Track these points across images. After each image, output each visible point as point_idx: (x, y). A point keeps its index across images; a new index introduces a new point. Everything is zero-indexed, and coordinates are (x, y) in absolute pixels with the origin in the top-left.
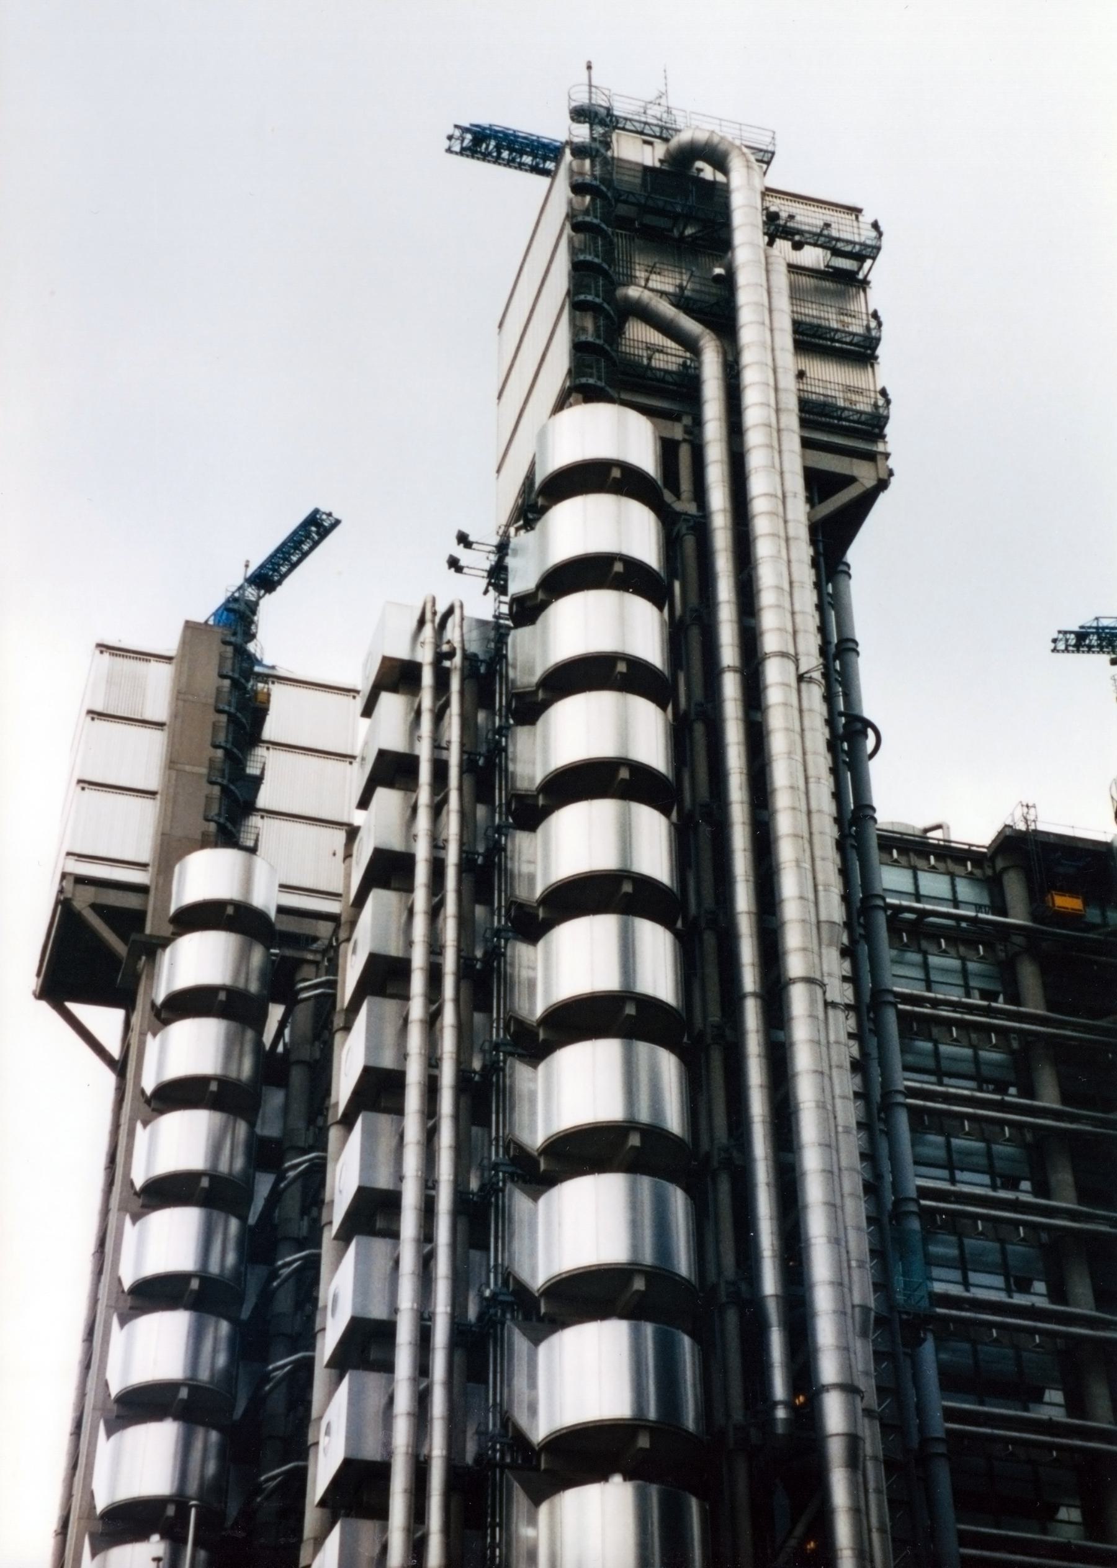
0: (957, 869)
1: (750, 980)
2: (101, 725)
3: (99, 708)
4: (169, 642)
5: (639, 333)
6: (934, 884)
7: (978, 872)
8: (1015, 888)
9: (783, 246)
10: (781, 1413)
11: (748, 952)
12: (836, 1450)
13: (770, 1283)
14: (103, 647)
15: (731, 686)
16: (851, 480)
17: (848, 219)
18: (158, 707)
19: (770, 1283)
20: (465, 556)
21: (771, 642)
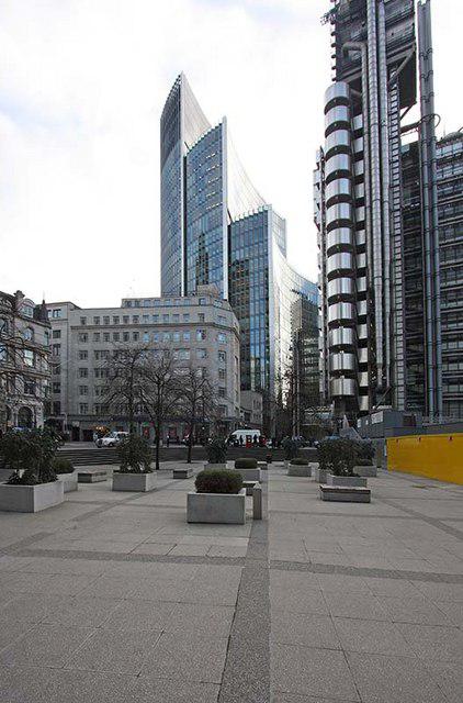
5: (351, 53)
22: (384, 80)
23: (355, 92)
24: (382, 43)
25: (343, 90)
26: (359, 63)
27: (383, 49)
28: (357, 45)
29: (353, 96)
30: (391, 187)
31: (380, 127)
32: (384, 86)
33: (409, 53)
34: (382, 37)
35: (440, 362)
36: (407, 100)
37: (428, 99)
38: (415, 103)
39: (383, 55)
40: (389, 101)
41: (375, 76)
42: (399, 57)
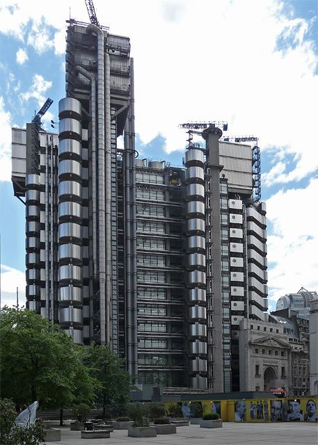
9: (110, 51)
11: (94, 205)
17: (125, 41)
21: (100, 147)
22: (109, 117)
23: (84, 110)
24: (108, 87)
25: (75, 106)
26: (89, 88)
27: (109, 92)
28: (88, 74)
29: (82, 112)
31: (106, 153)
32: (109, 121)
33: (125, 104)
34: (108, 82)
39: (108, 96)
40: (111, 131)
41: (104, 114)
42: (118, 102)
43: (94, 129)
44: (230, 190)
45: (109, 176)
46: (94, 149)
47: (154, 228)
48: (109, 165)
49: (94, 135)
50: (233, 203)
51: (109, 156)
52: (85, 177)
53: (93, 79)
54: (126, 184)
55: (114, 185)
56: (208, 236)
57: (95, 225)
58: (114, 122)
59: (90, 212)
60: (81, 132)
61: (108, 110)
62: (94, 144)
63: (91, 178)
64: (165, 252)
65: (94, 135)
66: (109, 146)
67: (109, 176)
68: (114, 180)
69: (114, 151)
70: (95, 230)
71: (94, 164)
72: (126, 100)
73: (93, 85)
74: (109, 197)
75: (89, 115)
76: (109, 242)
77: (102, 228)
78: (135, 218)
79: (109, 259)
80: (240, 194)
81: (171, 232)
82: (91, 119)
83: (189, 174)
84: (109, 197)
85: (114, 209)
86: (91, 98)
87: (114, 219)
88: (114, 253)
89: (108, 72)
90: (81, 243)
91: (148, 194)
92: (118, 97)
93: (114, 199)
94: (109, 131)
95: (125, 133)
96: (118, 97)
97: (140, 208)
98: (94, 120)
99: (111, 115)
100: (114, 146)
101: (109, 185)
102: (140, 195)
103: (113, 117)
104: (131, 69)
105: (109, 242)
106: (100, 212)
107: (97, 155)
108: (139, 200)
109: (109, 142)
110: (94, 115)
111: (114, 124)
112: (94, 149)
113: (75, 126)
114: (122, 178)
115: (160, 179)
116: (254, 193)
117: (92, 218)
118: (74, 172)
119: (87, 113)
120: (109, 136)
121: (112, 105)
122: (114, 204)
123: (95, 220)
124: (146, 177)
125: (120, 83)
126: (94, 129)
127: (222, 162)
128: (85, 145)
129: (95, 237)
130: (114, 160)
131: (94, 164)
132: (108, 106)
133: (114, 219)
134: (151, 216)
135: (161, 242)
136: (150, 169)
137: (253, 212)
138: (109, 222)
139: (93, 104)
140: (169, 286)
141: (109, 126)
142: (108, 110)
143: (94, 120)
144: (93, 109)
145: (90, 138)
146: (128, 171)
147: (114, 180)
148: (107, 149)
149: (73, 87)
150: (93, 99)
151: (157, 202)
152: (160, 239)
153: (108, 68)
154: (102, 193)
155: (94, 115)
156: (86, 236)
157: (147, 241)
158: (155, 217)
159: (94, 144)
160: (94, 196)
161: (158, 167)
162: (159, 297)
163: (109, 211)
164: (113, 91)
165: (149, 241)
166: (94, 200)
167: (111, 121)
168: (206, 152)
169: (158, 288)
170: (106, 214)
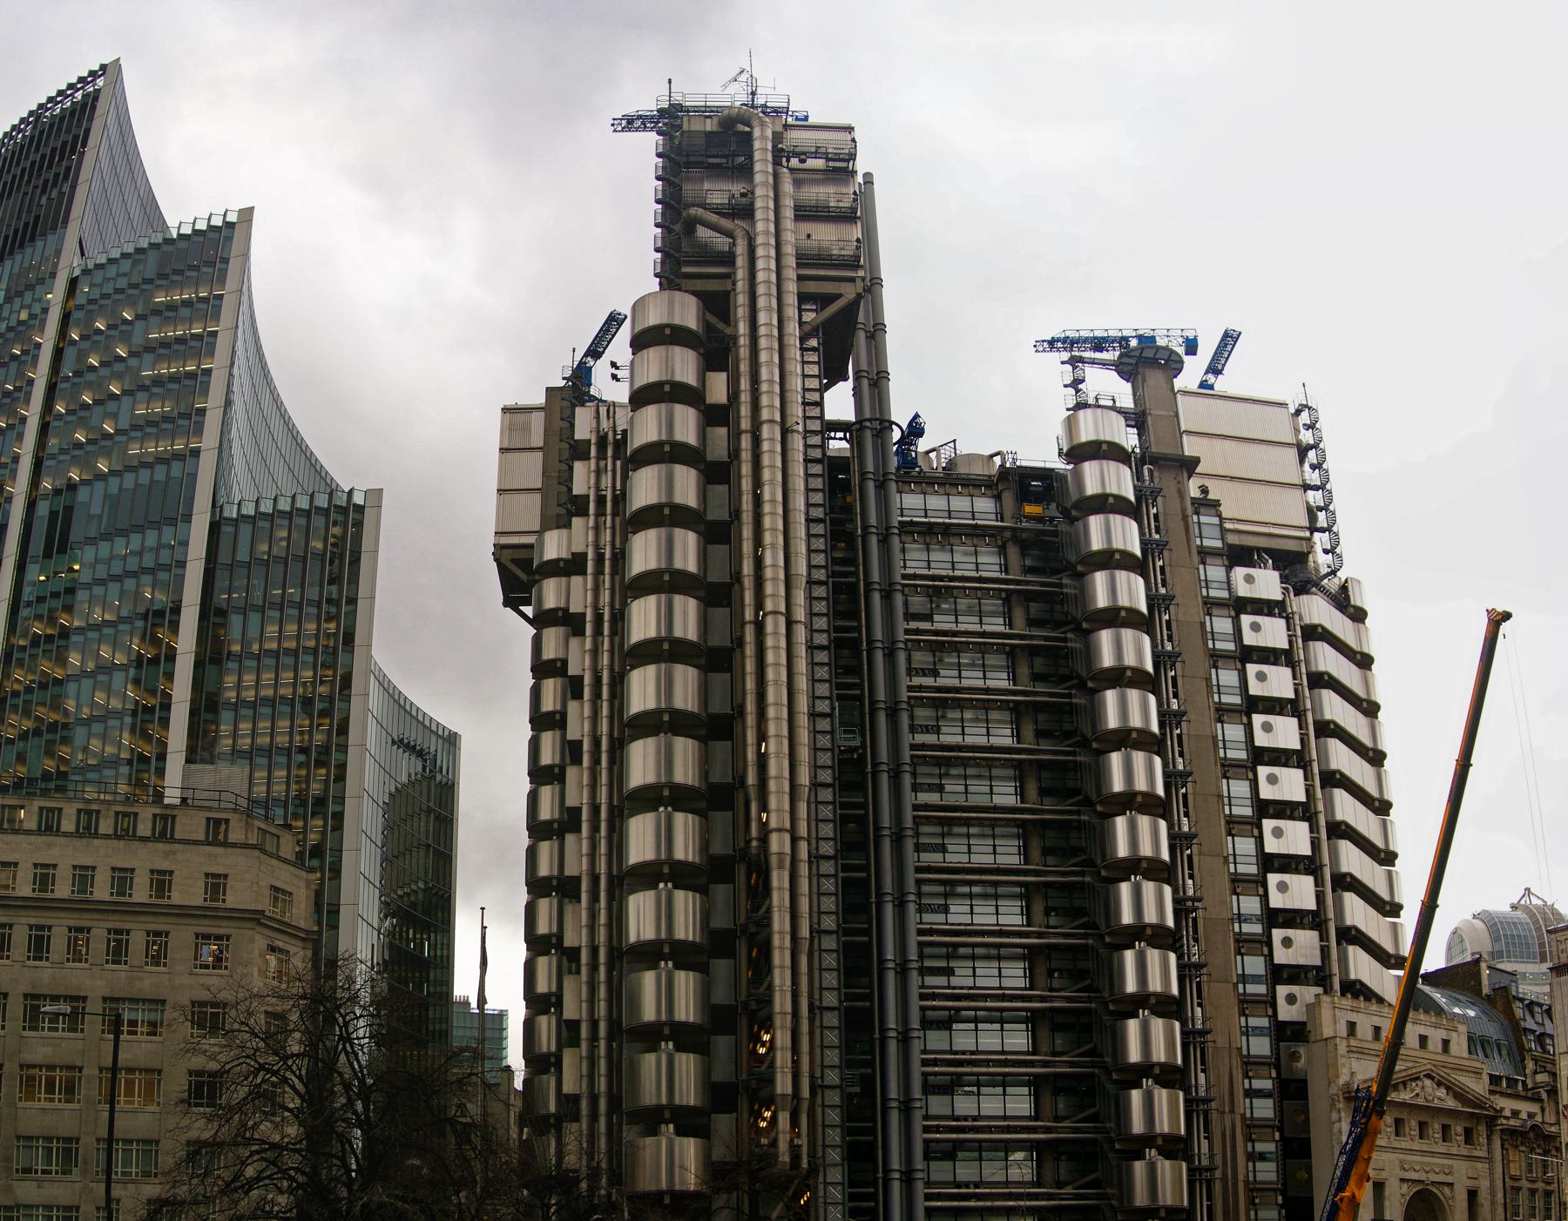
0: (976, 492)
1: (749, 615)
2: (510, 455)
3: (506, 446)
4: (540, 399)
6: (960, 503)
7: (989, 492)
8: (1008, 498)
10: (754, 843)
12: (774, 860)
13: (751, 779)
14: (505, 410)
15: (746, 442)
16: (840, 296)
18: (537, 439)
19: (751, 779)
20: (620, 374)
22: (793, 329)
23: (713, 320)
24: (789, 250)
25: (687, 312)
27: (790, 261)
30: (811, 583)
31: (785, 431)
32: (793, 340)
33: (849, 292)
34: (789, 237)
35: (917, 1092)
36: (833, 374)
37: (874, 385)
38: (846, 379)
39: (791, 274)
40: (802, 369)
43: (744, 367)
44: (1232, 539)
45: (799, 502)
46: (745, 424)
47: (973, 666)
48: (798, 469)
49: (744, 384)
50: (1249, 579)
51: (797, 443)
52: (718, 513)
53: (739, 234)
54: (865, 527)
55: (819, 529)
56: (1166, 688)
57: (750, 666)
58: (814, 343)
59: (738, 622)
60: (702, 379)
61: (791, 312)
62: (745, 410)
63: (736, 514)
64: (1019, 751)
65: (744, 384)
66: (796, 411)
67: (799, 502)
68: (818, 513)
69: (815, 426)
70: (750, 684)
71: (746, 469)
72: (852, 280)
73: (741, 249)
74: (801, 567)
75: (728, 331)
76: (803, 720)
77: (775, 674)
78: (902, 636)
79: (804, 778)
80: (1271, 552)
81: (1036, 678)
82: (735, 342)
83: (1080, 484)
84: (801, 567)
85: (821, 607)
86: (734, 284)
87: (821, 639)
88: (825, 759)
89: (788, 213)
90: (703, 732)
91: (947, 557)
92: (822, 272)
93: (820, 575)
94: (795, 368)
95: (857, 374)
96: (822, 272)
97: (918, 603)
98: (743, 341)
99: (801, 323)
100: (815, 412)
101: (800, 531)
102: (915, 560)
103: (807, 328)
104: (866, 193)
105: (803, 720)
106: (769, 620)
107: (756, 441)
108: (915, 577)
109: (796, 398)
110: (743, 328)
111: (814, 349)
112: (745, 424)
113: (684, 366)
114: (849, 509)
115: (985, 505)
116: (1318, 549)
117: (740, 643)
118: (678, 499)
119: (721, 326)
120: (796, 384)
121: (803, 298)
122: (820, 591)
123: (750, 650)
124: (936, 502)
125: (825, 235)
126: (744, 367)
127: (1190, 447)
128: (714, 416)
129: (750, 707)
130: (817, 454)
131: (746, 469)
132: (791, 300)
133: (821, 639)
134: (962, 627)
135: (1006, 715)
136: (952, 478)
137: (1316, 609)
138: (801, 651)
139: (742, 299)
140: (1037, 873)
141: (794, 353)
142: (791, 312)
143: (743, 341)
144: (742, 312)
145: (734, 395)
146: (871, 486)
147: (818, 513)
148: (790, 421)
149: (679, 263)
150: (741, 286)
151: (980, 580)
152: (1004, 705)
153: (788, 203)
154: (773, 558)
155: (743, 328)
156: (719, 706)
157: (950, 714)
158: (977, 628)
159: (745, 410)
160: (747, 568)
161: (978, 470)
162: (1003, 920)
163: (800, 614)
164: (803, 260)
165: (956, 714)
166: (748, 583)
167: (802, 340)
168: (1137, 419)
169: (996, 884)
170: (790, 624)
